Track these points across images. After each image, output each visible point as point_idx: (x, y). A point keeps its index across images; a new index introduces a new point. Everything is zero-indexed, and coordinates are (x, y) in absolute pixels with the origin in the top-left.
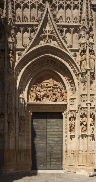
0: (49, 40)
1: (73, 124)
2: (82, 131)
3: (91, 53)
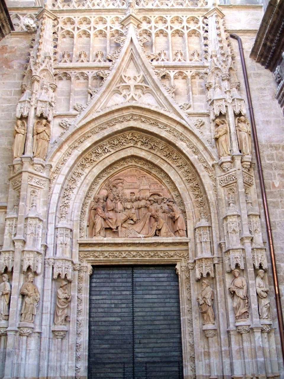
0: (136, 95)
1: (208, 296)
2: (237, 318)
3: (238, 119)
